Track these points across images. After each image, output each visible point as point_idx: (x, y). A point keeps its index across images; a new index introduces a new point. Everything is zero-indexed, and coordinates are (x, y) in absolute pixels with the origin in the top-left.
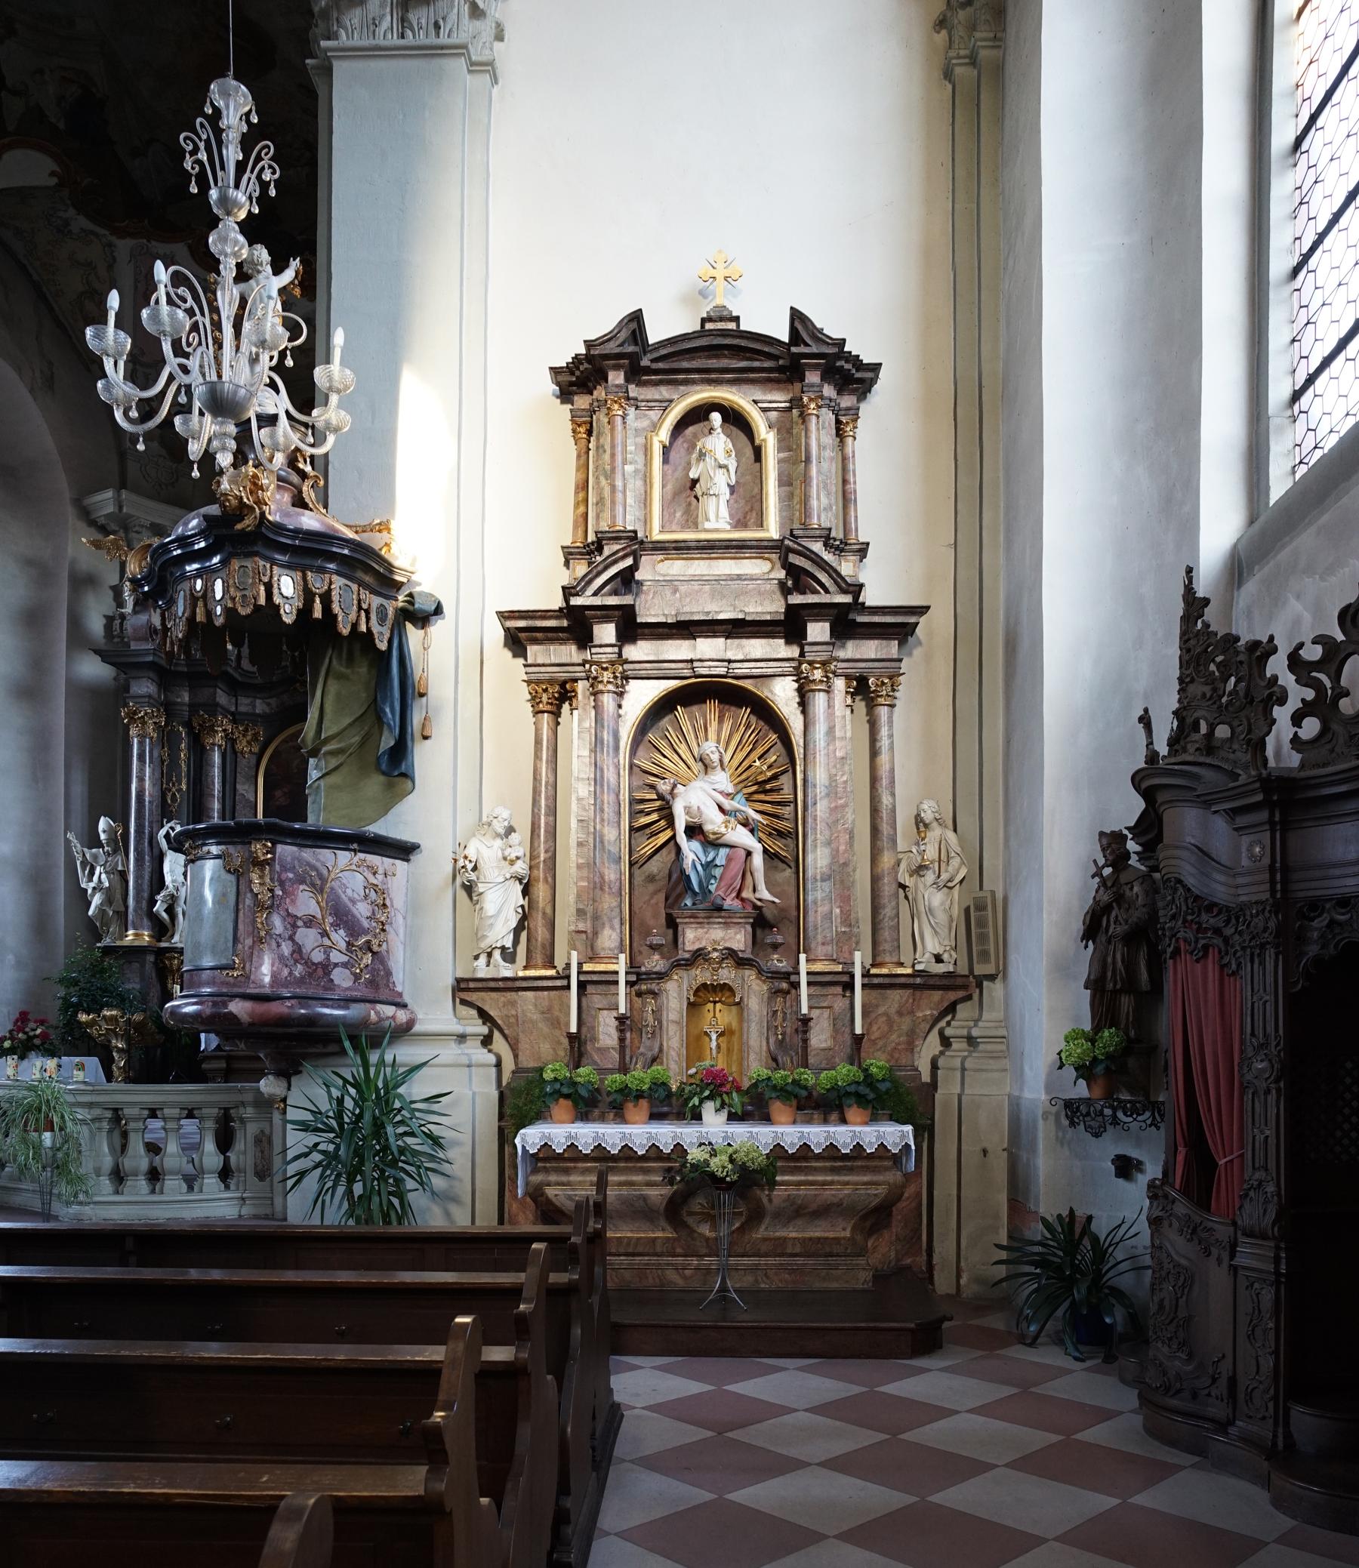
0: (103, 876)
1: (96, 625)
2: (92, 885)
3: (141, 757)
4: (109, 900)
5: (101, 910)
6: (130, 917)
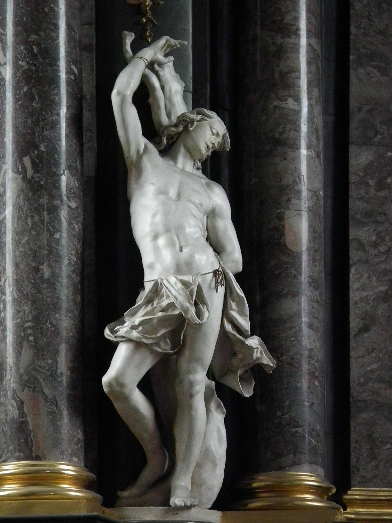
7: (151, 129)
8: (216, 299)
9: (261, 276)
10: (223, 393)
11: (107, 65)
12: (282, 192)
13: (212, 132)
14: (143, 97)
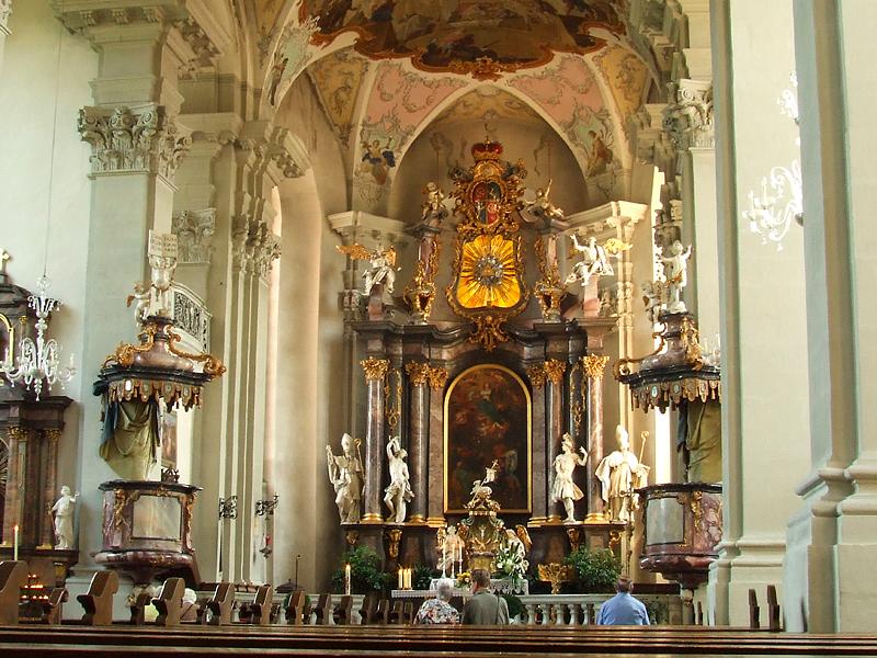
0: (347, 475)
1: (333, 300)
2: (340, 482)
3: (375, 394)
4: (352, 493)
7: (394, 454)
8: (404, 485)
9: (412, 480)
10: (406, 501)
12: (416, 464)
13: (404, 453)
14: (392, 448)
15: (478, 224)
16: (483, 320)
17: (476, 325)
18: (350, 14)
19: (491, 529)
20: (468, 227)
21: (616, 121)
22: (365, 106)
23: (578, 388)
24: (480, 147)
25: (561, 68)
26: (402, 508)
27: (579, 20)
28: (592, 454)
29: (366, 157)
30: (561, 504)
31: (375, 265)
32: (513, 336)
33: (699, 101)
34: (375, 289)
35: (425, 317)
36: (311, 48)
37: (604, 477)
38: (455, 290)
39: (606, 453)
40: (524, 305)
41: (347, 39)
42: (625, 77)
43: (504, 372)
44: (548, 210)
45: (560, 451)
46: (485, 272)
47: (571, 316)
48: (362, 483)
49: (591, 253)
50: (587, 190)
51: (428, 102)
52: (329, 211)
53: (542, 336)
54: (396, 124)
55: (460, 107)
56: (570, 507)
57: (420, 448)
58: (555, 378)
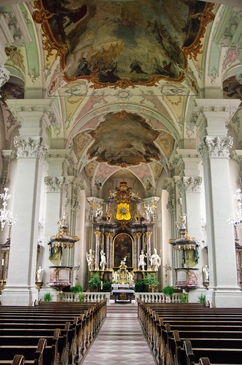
0: (91, 259)
1: (88, 217)
2: (89, 260)
3: (98, 240)
4: (92, 263)
5: (90, 265)
6: (96, 266)
9: (106, 260)
11: (100, 251)
13: (104, 254)
15: (121, 200)
16: (122, 222)
17: (120, 224)
18: (97, 153)
19: (125, 272)
20: (119, 201)
21: (153, 178)
22: (96, 173)
23: (145, 239)
24: (122, 183)
25: (142, 166)
26: (104, 267)
27: (148, 156)
28: (148, 255)
29: (96, 184)
30: (141, 267)
31: (98, 210)
32: (129, 227)
33: (187, 181)
34: (98, 215)
35: (109, 222)
36: (88, 160)
37: (151, 260)
38: (116, 215)
39: (152, 255)
40: (132, 220)
41: (95, 158)
42: (156, 169)
43: (128, 236)
44: (137, 198)
45: (141, 254)
46: (123, 212)
47: (143, 223)
48: (94, 261)
49: (148, 208)
50: (147, 193)
51: (110, 172)
52: (87, 197)
53: (136, 227)
54: (103, 177)
55: (117, 174)
56: (143, 267)
57: (108, 253)
58: (139, 237)
